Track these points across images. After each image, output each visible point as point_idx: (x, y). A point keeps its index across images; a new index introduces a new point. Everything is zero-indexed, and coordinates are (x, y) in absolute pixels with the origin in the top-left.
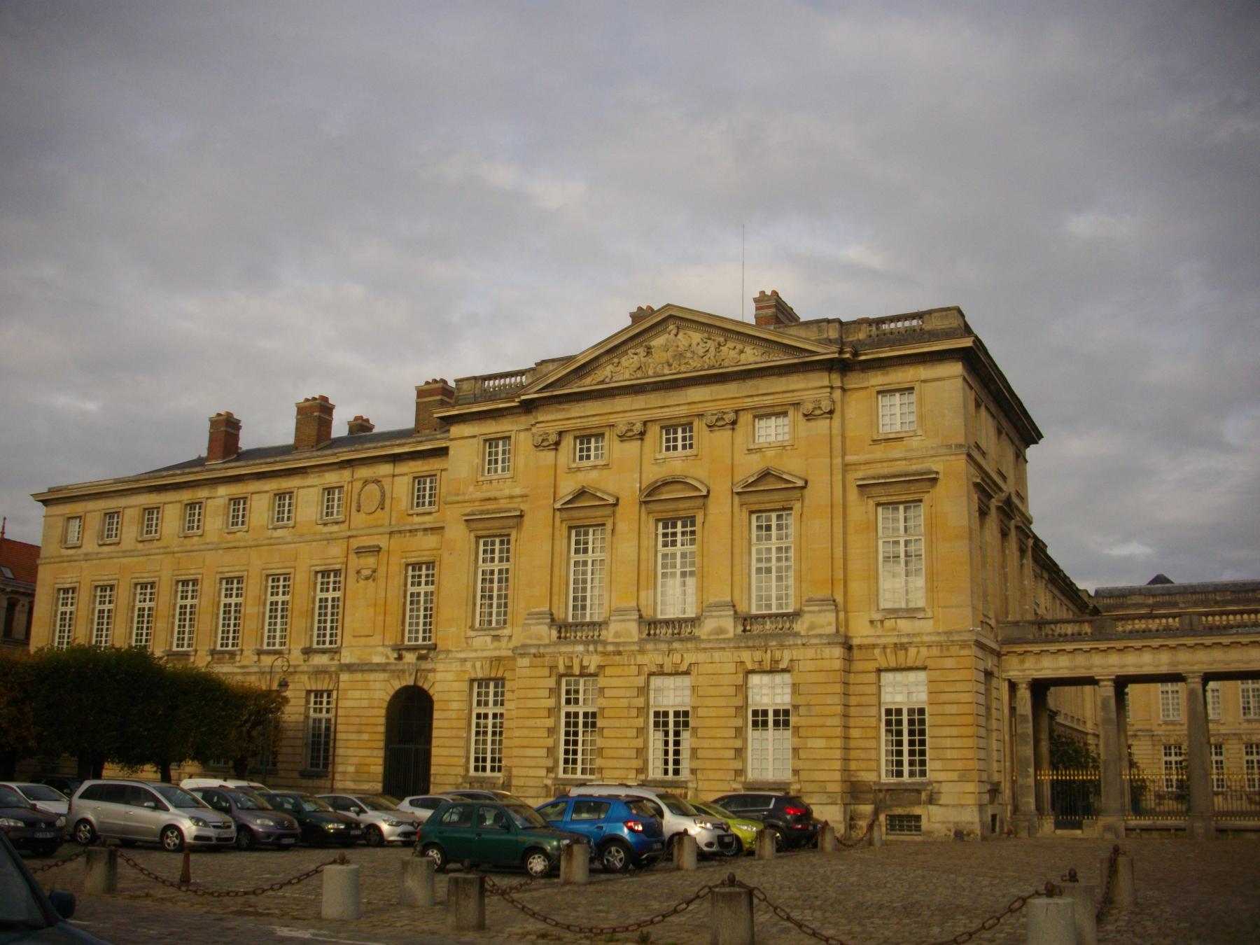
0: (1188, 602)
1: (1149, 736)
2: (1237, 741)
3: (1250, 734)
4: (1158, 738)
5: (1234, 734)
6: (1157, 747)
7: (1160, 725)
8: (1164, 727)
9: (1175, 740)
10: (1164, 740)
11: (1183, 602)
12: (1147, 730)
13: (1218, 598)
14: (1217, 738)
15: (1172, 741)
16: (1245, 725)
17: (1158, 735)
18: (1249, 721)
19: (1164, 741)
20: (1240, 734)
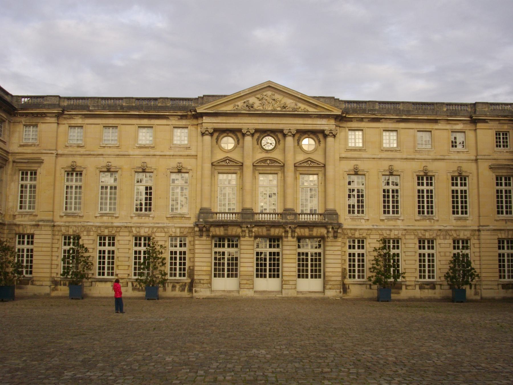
0: (98, 106)
1: (50, 226)
2: (127, 234)
3: (139, 227)
4: (58, 228)
5: (126, 227)
6: (57, 237)
7: (61, 217)
8: (65, 219)
9: (73, 231)
10: (63, 230)
11: (94, 106)
12: (48, 221)
13: (124, 104)
14: (110, 229)
15: (71, 232)
16: (136, 219)
17: (59, 226)
18: (139, 216)
19: (64, 231)
20: (131, 227)
